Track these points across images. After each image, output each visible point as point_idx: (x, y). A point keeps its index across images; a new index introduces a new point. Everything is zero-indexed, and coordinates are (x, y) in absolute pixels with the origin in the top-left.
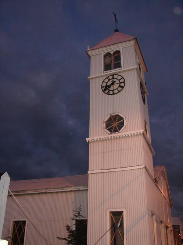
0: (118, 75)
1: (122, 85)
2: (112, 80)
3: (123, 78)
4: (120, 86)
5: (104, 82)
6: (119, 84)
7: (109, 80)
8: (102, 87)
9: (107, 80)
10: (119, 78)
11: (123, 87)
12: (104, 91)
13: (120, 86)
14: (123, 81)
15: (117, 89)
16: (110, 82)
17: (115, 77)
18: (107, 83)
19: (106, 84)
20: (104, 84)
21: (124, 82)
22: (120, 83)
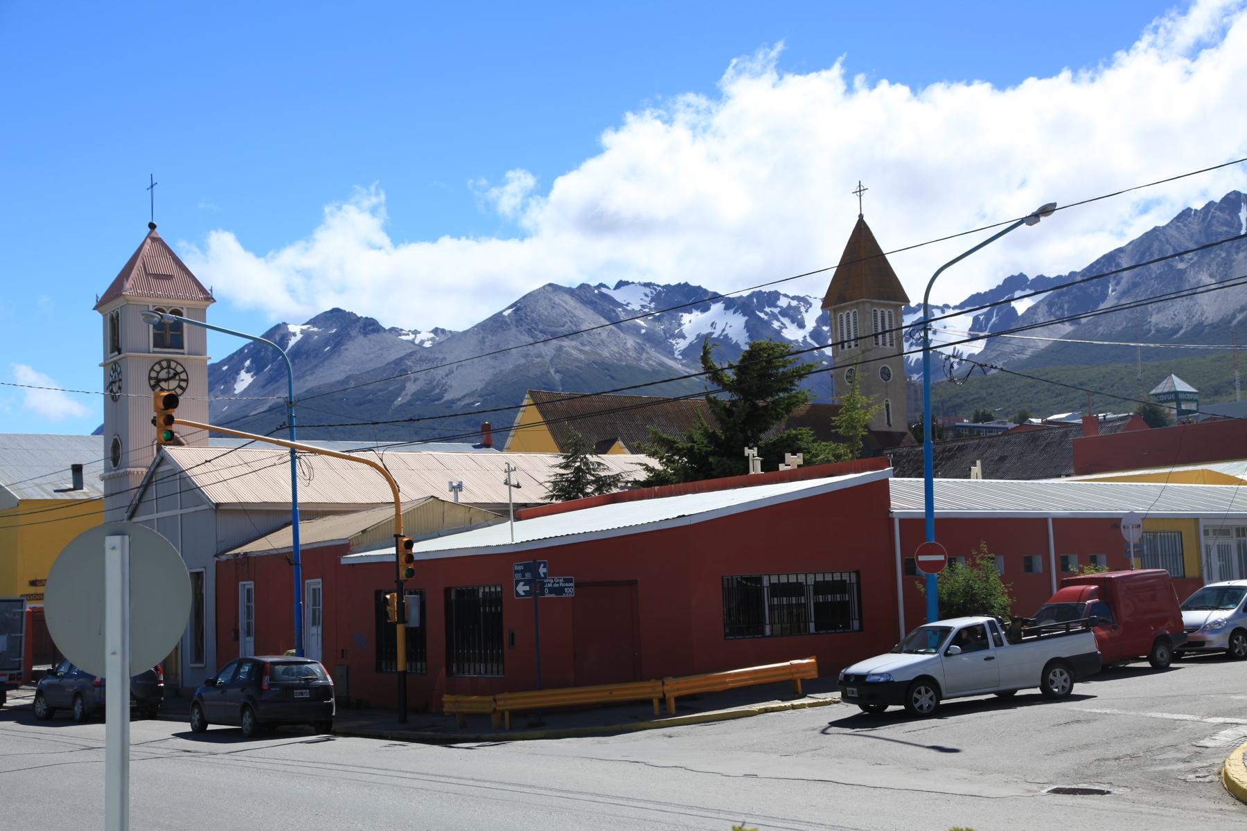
0: (178, 363)
1: (183, 384)
2: (166, 370)
3: (185, 371)
4: (179, 386)
5: (152, 369)
6: (178, 382)
7: (162, 368)
8: (150, 378)
9: (157, 368)
10: (179, 369)
11: (184, 389)
12: (153, 387)
13: (179, 386)
14: (185, 378)
15: (174, 389)
16: (163, 375)
17: (173, 365)
18: (158, 373)
19: (158, 375)
20: (153, 374)
21: (186, 381)
22: (181, 380)
